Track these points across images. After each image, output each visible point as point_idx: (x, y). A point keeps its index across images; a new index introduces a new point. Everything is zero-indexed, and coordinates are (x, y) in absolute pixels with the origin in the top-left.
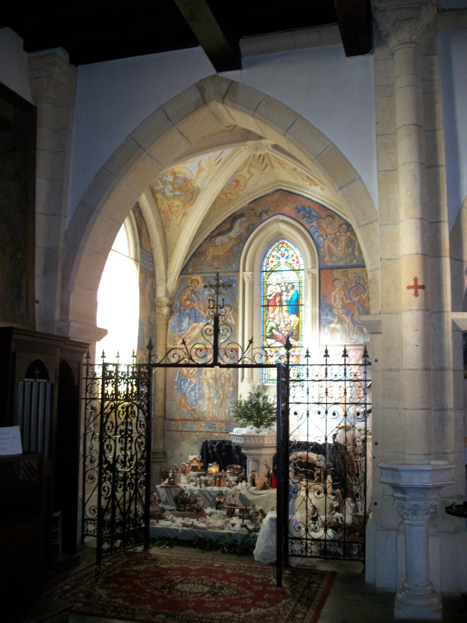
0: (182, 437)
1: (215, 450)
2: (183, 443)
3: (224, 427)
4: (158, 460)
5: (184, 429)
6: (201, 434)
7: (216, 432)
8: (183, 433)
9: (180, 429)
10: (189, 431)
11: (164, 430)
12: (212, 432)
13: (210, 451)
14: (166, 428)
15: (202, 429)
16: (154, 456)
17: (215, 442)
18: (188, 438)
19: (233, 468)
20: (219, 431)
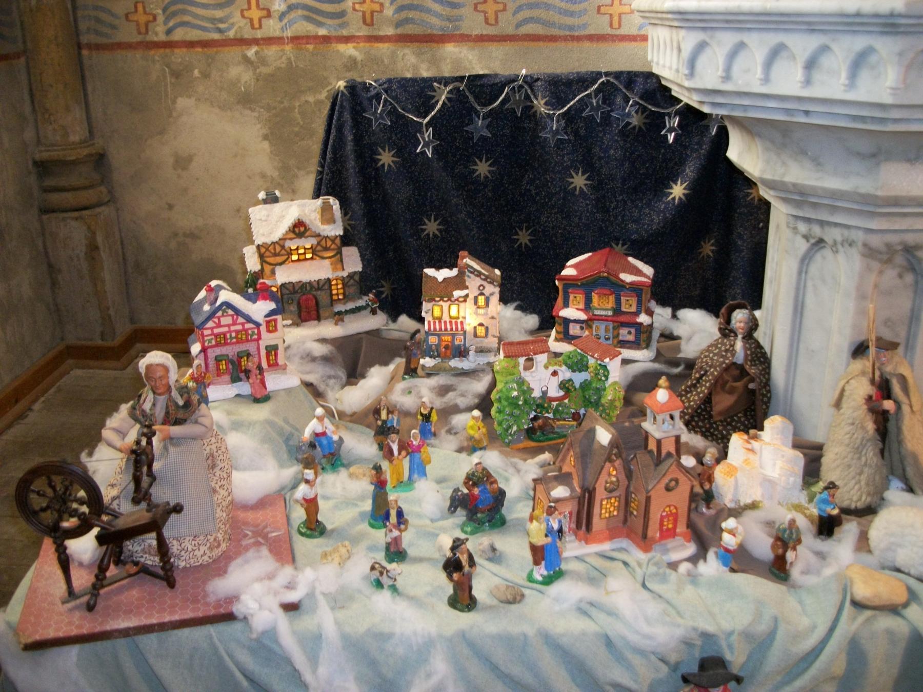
0: (176, 75)
1: (426, 144)
2: (182, 102)
3: (389, 11)
4: (68, 198)
5: (179, 35)
6: (271, 52)
7: (347, 39)
8: (179, 55)
9: (162, 37)
10: (205, 44)
11: (79, 47)
12: (326, 39)
13: (386, 158)
14: (84, 39)
15: (272, 27)
16: (50, 182)
17: (419, 92)
18: (206, 75)
19: (617, 288)
20: (364, 31)
